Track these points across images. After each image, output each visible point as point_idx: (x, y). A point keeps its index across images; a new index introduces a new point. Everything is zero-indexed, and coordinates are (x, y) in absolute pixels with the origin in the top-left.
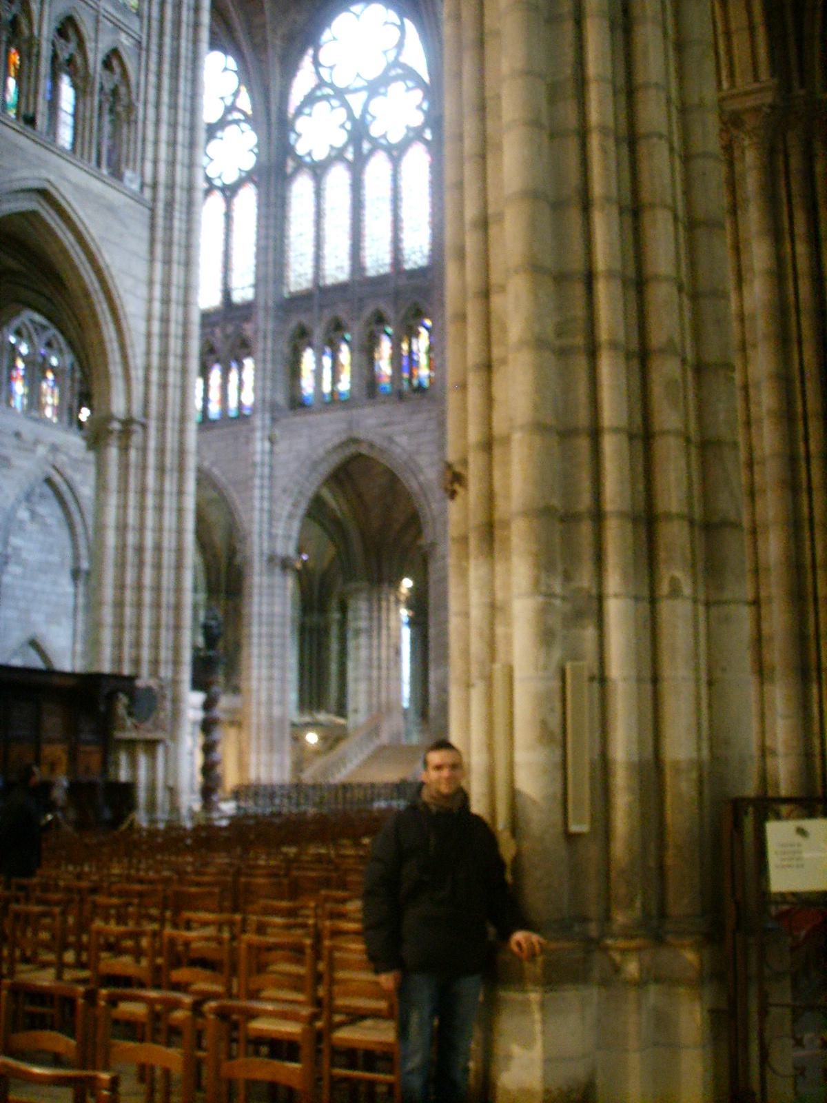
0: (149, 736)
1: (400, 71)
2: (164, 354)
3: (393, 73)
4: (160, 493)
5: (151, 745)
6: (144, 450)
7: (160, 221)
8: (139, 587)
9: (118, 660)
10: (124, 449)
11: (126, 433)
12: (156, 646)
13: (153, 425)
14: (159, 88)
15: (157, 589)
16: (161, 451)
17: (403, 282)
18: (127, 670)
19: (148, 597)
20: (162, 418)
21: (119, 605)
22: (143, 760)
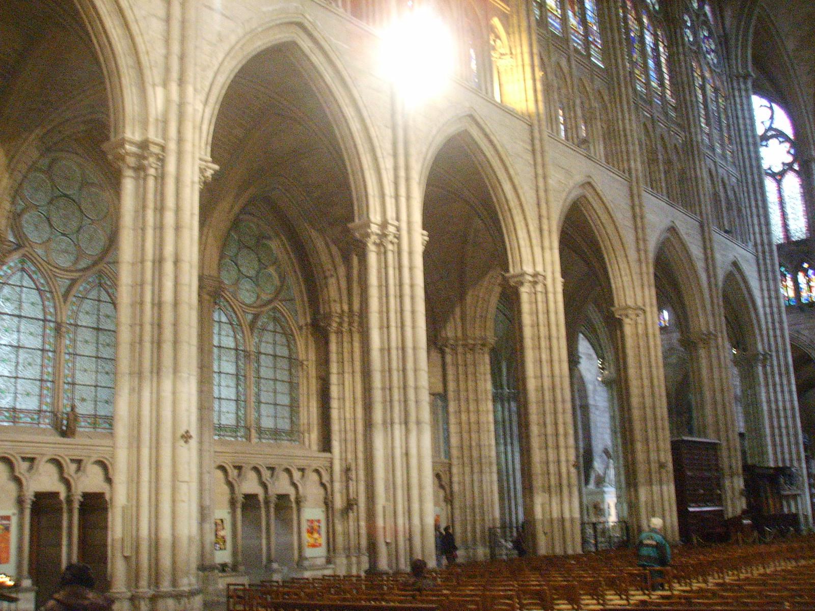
1: (774, 133)
2: (773, 323)
3: (769, 134)
4: (782, 385)
5: (795, 497)
6: (772, 366)
7: (761, 261)
8: (780, 427)
9: (776, 461)
10: (764, 367)
11: (765, 359)
13: (774, 354)
14: (749, 199)
15: (787, 427)
17: (792, 247)
19: (784, 431)
20: (777, 351)
21: (773, 435)
22: (793, 504)
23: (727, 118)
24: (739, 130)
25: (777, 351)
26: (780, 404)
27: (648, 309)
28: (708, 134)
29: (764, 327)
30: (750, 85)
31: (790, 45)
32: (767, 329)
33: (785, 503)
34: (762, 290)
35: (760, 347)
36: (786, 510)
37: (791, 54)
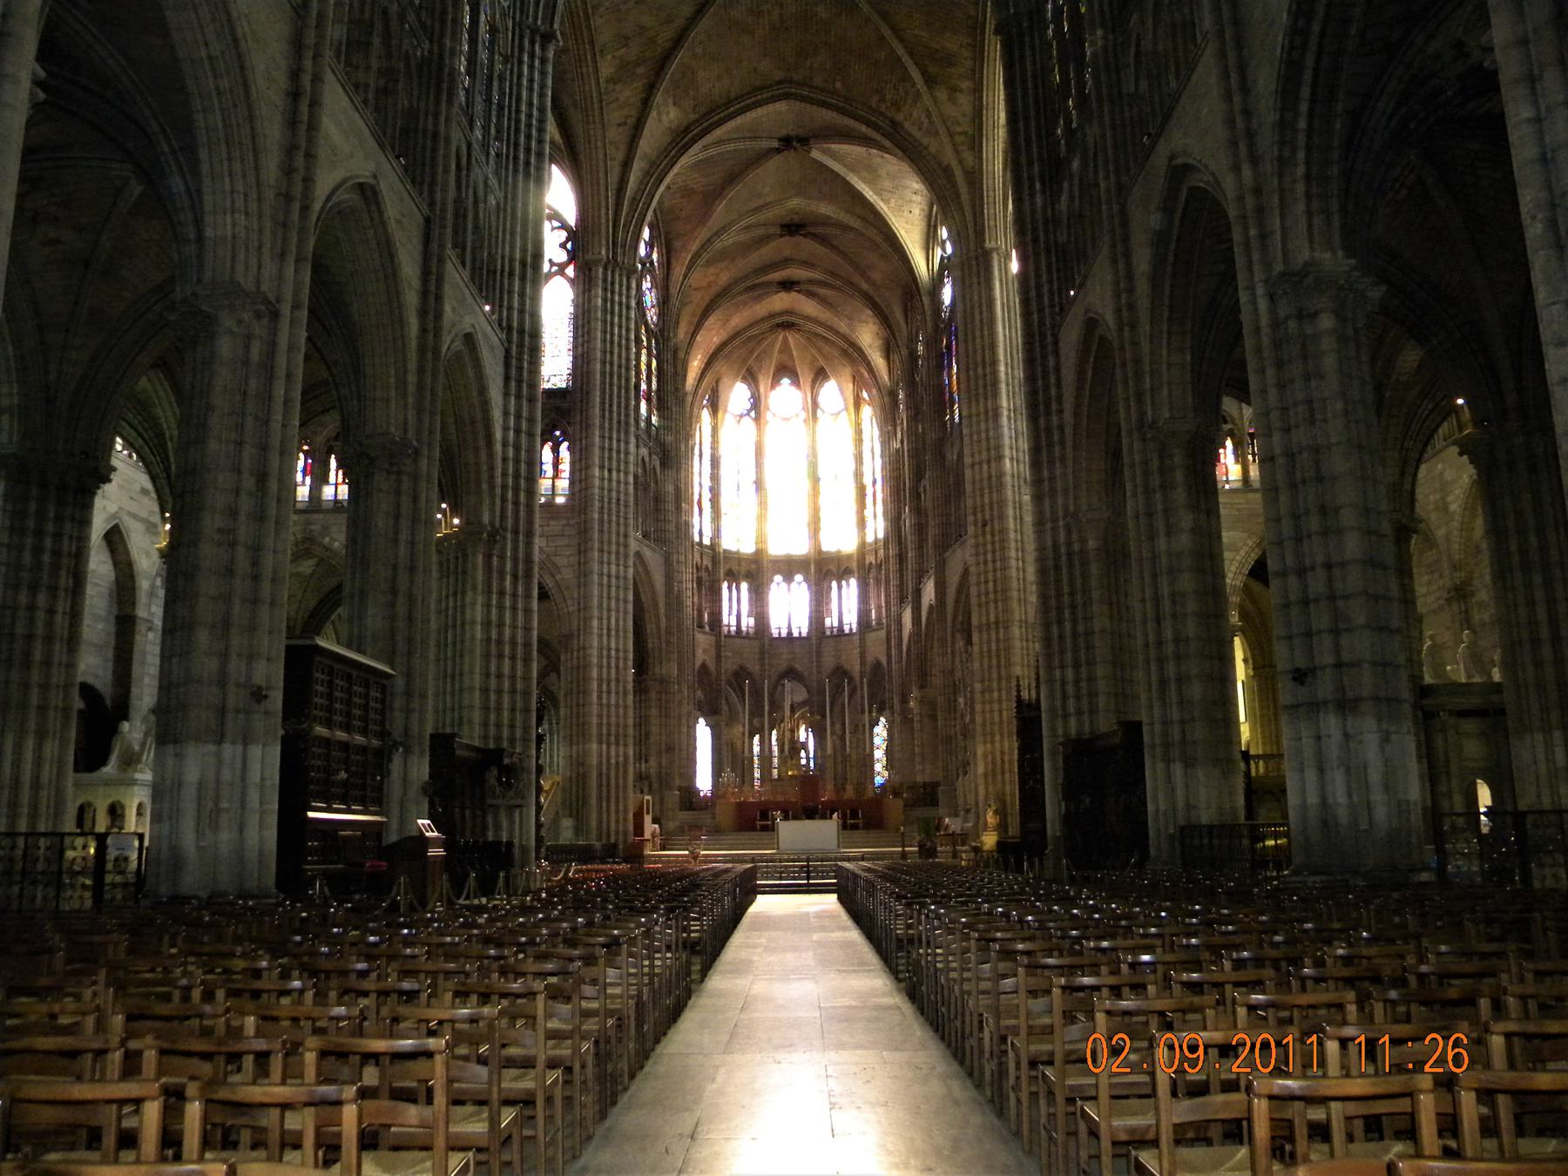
0: (513, 802)
4: (514, 595)
6: (502, 557)
8: (500, 676)
9: (485, 738)
10: (488, 557)
12: (512, 727)
13: (509, 536)
15: (513, 677)
16: (515, 559)
18: (492, 746)
20: (516, 532)
21: (485, 691)
23: (502, 93)
24: (518, 121)
25: (516, 532)
26: (507, 632)
27: (286, 309)
28: (467, 91)
29: (499, 481)
30: (551, 54)
31: (606, 69)
32: (505, 487)
33: (490, 819)
34: (506, 414)
35: (486, 519)
36: (490, 836)
37: (603, 85)
